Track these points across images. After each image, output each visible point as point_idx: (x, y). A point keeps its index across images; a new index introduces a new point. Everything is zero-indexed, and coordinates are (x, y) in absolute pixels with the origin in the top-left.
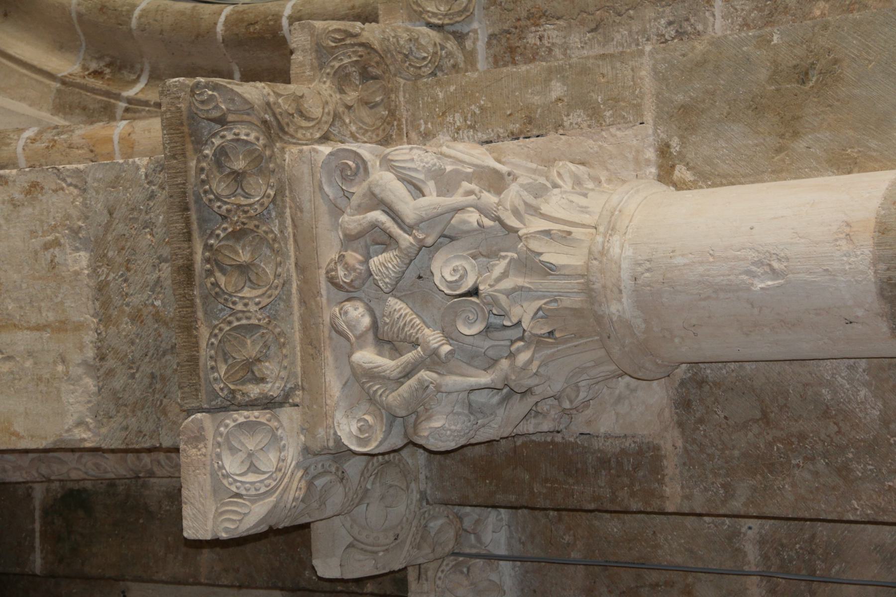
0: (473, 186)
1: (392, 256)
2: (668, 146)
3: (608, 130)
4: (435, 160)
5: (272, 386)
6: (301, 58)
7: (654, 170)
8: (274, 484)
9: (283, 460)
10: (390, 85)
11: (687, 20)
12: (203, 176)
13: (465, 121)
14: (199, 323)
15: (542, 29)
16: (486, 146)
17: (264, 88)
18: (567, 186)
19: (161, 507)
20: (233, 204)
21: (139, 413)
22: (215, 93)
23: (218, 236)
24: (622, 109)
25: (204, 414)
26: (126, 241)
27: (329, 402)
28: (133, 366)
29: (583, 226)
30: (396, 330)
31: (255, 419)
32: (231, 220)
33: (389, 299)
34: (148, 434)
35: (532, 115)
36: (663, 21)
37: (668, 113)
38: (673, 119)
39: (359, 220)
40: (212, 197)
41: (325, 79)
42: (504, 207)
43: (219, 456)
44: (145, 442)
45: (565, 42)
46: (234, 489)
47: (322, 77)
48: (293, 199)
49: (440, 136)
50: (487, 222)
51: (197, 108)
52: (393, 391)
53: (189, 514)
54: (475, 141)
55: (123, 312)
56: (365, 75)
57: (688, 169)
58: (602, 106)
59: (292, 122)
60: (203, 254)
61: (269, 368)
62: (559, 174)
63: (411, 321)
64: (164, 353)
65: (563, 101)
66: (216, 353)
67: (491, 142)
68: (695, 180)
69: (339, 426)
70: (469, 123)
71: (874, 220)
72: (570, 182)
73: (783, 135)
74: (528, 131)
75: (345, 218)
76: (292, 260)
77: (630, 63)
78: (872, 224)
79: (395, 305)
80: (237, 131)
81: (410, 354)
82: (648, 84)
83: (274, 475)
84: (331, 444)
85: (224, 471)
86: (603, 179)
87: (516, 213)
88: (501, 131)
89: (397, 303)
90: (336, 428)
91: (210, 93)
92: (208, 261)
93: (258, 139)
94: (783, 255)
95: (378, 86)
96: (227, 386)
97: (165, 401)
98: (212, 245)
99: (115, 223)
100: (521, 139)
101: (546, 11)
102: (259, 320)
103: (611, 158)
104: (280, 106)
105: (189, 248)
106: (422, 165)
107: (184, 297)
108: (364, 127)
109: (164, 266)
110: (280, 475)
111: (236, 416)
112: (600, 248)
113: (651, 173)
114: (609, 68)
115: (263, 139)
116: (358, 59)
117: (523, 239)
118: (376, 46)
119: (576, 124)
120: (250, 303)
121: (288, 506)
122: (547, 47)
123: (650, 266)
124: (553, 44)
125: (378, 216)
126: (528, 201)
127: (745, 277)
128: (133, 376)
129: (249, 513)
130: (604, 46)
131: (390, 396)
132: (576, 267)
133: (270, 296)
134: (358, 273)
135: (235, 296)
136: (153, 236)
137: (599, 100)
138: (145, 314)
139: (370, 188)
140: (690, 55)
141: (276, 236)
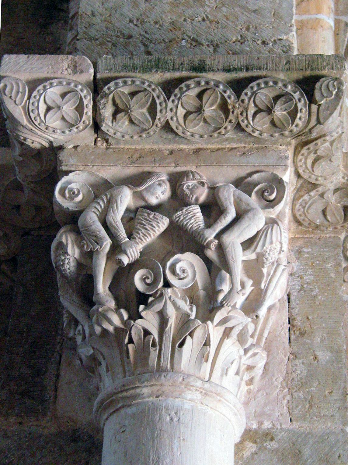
1: (200, 223)
2: (272, 439)
5: (109, 126)
7: (255, 426)
9: (54, 131)
10: (339, 227)
12: (271, 83)
13: (307, 283)
14: (162, 74)
16: (286, 298)
18: (246, 361)
19: (49, 34)
20: (248, 104)
21: (104, 24)
22: (333, 97)
23: (225, 92)
24: (304, 406)
26: (232, 22)
27: (95, 168)
28: (139, 22)
30: (144, 222)
31: (85, 112)
32: (237, 102)
33: (168, 219)
34: (87, 31)
35: (306, 335)
37: (297, 441)
38: (291, 445)
39: (229, 199)
40: (255, 89)
41: (346, 178)
42: (230, 311)
43: (60, 83)
44: (81, 28)
46: (33, 95)
49: (297, 263)
50: (221, 297)
51: (324, 82)
52: (98, 217)
53: (20, 59)
54: (291, 289)
55: (180, 17)
57: (252, 453)
58: (307, 390)
59: (311, 152)
60: (213, 80)
61: (123, 124)
62: (255, 355)
64: (146, 46)
66: (137, 86)
67: (289, 302)
69: (76, 174)
70: (305, 286)
72: (249, 362)
75: (232, 188)
76: (205, 146)
77: (338, 414)
79: (163, 223)
80: (304, 111)
82: (320, 427)
83: (43, 124)
84: (64, 168)
85: (48, 87)
86: (252, 387)
87: (225, 321)
88: (296, 311)
89: (164, 224)
91: (334, 93)
92: (207, 83)
93: (297, 126)
95: (339, 218)
96: (112, 92)
97: (110, 45)
98: (218, 87)
99: (247, 14)
100: (289, 326)
102: (159, 119)
103: (267, 394)
104: (322, 144)
105: (218, 70)
106: (268, 250)
107: (182, 64)
108: (307, 206)
109: (211, 49)
110: (43, 128)
111: (89, 98)
112: (192, 384)
113: (252, 424)
114: (336, 398)
115: (297, 130)
117: (204, 324)
119: (296, 369)
120: (173, 113)
121: (20, 134)
123: (174, 421)
125: (231, 215)
126: (234, 329)
128: (131, 21)
129: (16, 104)
131: (94, 215)
132: (180, 362)
134: (189, 196)
135: (178, 102)
136: (234, 42)
137: (312, 389)
138: (176, 33)
139: (256, 208)
140: (339, 462)
141: (224, 135)
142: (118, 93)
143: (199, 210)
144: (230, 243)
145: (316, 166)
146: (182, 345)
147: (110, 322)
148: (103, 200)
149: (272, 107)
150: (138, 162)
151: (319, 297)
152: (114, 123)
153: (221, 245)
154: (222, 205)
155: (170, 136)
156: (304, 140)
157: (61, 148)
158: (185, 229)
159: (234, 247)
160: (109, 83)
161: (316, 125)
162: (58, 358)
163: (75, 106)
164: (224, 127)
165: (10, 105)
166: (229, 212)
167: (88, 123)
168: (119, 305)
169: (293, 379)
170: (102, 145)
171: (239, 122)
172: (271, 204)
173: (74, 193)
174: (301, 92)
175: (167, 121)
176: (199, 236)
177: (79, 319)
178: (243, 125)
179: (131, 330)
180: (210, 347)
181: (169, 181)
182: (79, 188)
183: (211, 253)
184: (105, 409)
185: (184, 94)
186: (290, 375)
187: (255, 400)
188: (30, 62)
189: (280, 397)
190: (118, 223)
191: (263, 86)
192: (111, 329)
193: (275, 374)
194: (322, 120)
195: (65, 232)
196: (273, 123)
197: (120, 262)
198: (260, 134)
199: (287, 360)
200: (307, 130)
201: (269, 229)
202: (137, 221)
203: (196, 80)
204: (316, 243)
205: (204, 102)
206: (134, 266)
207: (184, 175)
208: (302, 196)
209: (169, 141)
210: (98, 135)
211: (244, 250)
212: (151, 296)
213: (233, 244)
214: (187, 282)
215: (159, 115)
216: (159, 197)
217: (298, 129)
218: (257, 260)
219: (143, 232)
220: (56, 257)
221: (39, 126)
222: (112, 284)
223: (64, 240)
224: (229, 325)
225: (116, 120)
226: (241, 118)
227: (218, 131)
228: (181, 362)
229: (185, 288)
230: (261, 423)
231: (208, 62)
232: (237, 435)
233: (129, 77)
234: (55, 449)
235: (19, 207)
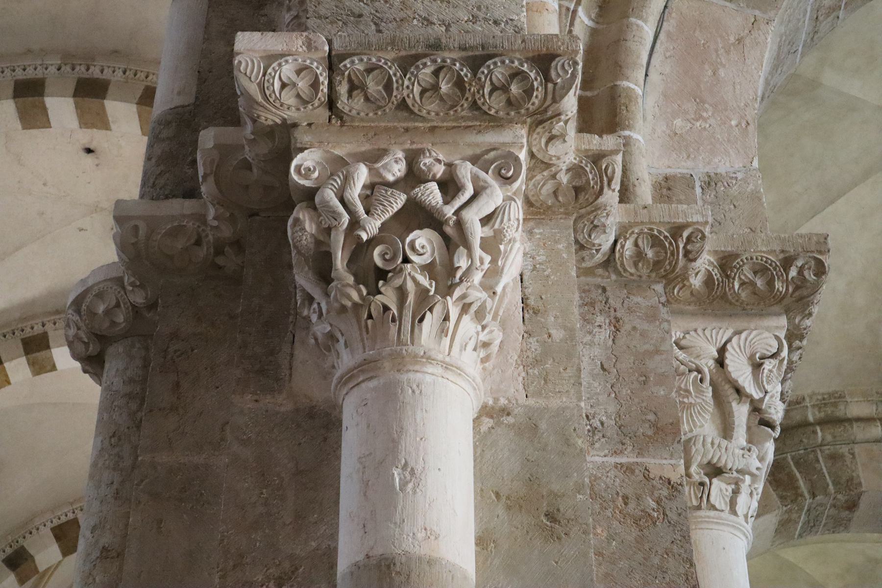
0: (486, 266)
1: (438, 199)
2: (508, 414)
3: (524, 371)
4: (509, 238)
6: (595, 142)
7: (491, 402)
8: (271, 100)
9: (288, 108)
11: (603, 437)
12: (507, 61)
13: (540, 264)
14: (397, 52)
15: (607, 327)
17: (572, 112)
18: (483, 337)
19: (263, 16)
22: (569, 75)
23: (462, 70)
25: (328, 51)
27: (330, 145)
29: (451, 346)
32: (473, 80)
33: (405, 196)
34: (317, 9)
35: (539, 314)
36: (604, 418)
39: (466, 177)
40: (492, 67)
41: (578, 159)
42: (469, 287)
45: (595, 345)
46: (269, 71)
47: (579, 157)
48: (487, 128)
49: (529, 244)
50: (459, 274)
51: (559, 62)
52: (336, 194)
53: (254, 36)
54: (523, 269)
56: (578, 190)
57: (489, 428)
59: (546, 131)
60: (449, 58)
61: (358, 102)
62: (491, 332)
63: (388, 211)
64: (376, 24)
65: (549, 338)
67: (522, 282)
68: (480, 433)
69: (311, 152)
70: (538, 266)
71: (438, 557)
73: (509, 498)
74: (528, 311)
75: (469, 165)
76: (440, 124)
77: (573, 391)
78: (435, 555)
79: (399, 201)
82: (555, 403)
83: (278, 101)
84: (299, 145)
85: (284, 64)
86: (487, 365)
87: (464, 296)
88: (530, 290)
89: (402, 201)
91: (570, 72)
92: (444, 61)
94: (418, 490)
96: (347, 69)
97: (340, 23)
98: (455, 65)
100: (522, 305)
101: (619, 331)
102: (396, 97)
103: (502, 371)
104: (557, 123)
105: (454, 48)
106: (506, 227)
107: (418, 41)
109: (443, 29)
110: (278, 105)
114: (570, 374)
115: (533, 109)
116: (592, 185)
117: (444, 300)
118: (601, 200)
121: (254, 111)
122: (593, 331)
123: (416, 393)
124: (594, 335)
126: (472, 305)
127: (403, 461)
129: (251, 81)
130: (590, 373)
132: (420, 338)
133: (413, 105)
135: (415, 79)
136: (466, 22)
137: (547, 366)
138: (408, 12)
142: (354, 70)
143: (437, 187)
145: (550, 145)
146: (421, 320)
147: (349, 297)
148: (339, 177)
149: (509, 85)
150: (373, 139)
151: (552, 277)
152: (350, 100)
154: (460, 183)
155: (406, 114)
156: (539, 119)
157: (295, 125)
160: (345, 59)
161: (552, 104)
162: (292, 339)
163: (311, 83)
165: (243, 81)
167: (323, 100)
168: (358, 281)
169: (528, 357)
170: (336, 122)
172: (507, 180)
173: (310, 170)
174: (536, 70)
175: (404, 98)
176: (437, 213)
177: (316, 296)
178: (479, 102)
179: (370, 305)
181: (405, 158)
182: (314, 165)
183: (449, 230)
184: (345, 383)
185: (421, 72)
188: (263, 40)
189: (516, 374)
190: (355, 200)
191: (499, 64)
192: (349, 304)
193: (510, 352)
194: (558, 99)
195: (301, 208)
196: (509, 103)
197: (359, 237)
198: (497, 112)
200: (542, 109)
202: (374, 197)
203: (432, 57)
204: (547, 225)
205: (440, 80)
206: (373, 242)
207: (420, 152)
208: (535, 176)
209: (405, 120)
211: (482, 226)
213: (472, 220)
214: (426, 259)
215: (395, 93)
217: (535, 107)
220: (293, 233)
222: (349, 261)
223: (301, 217)
224: (468, 301)
225: (351, 98)
226: (477, 96)
227: (455, 109)
229: (424, 263)
230: (496, 400)
231: (444, 41)
232: (471, 415)
233: (365, 54)
234: (293, 426)
235: (247, 187)
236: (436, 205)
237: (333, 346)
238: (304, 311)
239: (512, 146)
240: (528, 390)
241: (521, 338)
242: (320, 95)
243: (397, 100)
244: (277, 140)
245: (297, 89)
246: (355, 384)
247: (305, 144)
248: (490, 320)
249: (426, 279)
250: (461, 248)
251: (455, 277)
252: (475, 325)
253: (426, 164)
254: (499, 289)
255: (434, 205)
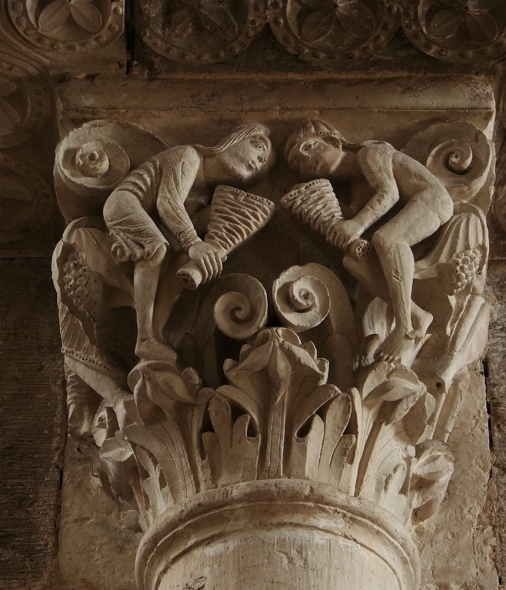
0: (424, 334)
5: (158, 36)
9: (52, 46)
27: (130, 114)
33: (272, 203)
39: (386, 169)
52: (141, 201)
62: (434, 459)
69: (95, 126)
76: (336, 76)
81: (192, 227)
86: (424, 524)
88: (502, 390)
89: (266, 213)
90: (93, 122)
100: (488, 416)
102: (253, 22)
103: (453, 536)
110: (32, 39)
126: (400, 405)
132: (302, 464)
144: (391, 246)
146: (304, 432)
153: (374, 249)
158: (305, 221)
159: (399, 253)
164: (373, 37)
166: (387, 190)
167: (117, 28)
171: (401, 28)
173: (92, 157)
175: (267, 25)
176: (332, 234)
178: (408, 32)
179: (208, 405)
180: (357, 438)
181: (270, 138)
186: (494, 503)
187: (432, 546)
190: (179, 211)
197: (188, 279)
198: (440, 53)
199: (488, 477)
201: (461, 222)
202: (214, 207)
210: (133, 54)
212: (244, 342)
213: (398, 247)
216: (253, 165)
218: (440, 280)
219: (228, 227)
220: (62, 274)
221: (24, 36)
224: (391, 396)
227: (363, 46)
228: (305, 462)
236: (330, 221)
237: (138, 487)
238: (81, 426)
239: (468, 114)
240: (503, 569)
241: (487, 475)
242: (110, 19)
243: (254, 29)
244: (29, 109)
245: (69, 9)
246: (180, 551)
247: (83, 112)
248: (431, 437)
249: (313, 357)
250: (377, 300)
251: (366, 354)
252: (403, 446)
253: (310, 146)
254: (448, 378)
255: (327, 219)
